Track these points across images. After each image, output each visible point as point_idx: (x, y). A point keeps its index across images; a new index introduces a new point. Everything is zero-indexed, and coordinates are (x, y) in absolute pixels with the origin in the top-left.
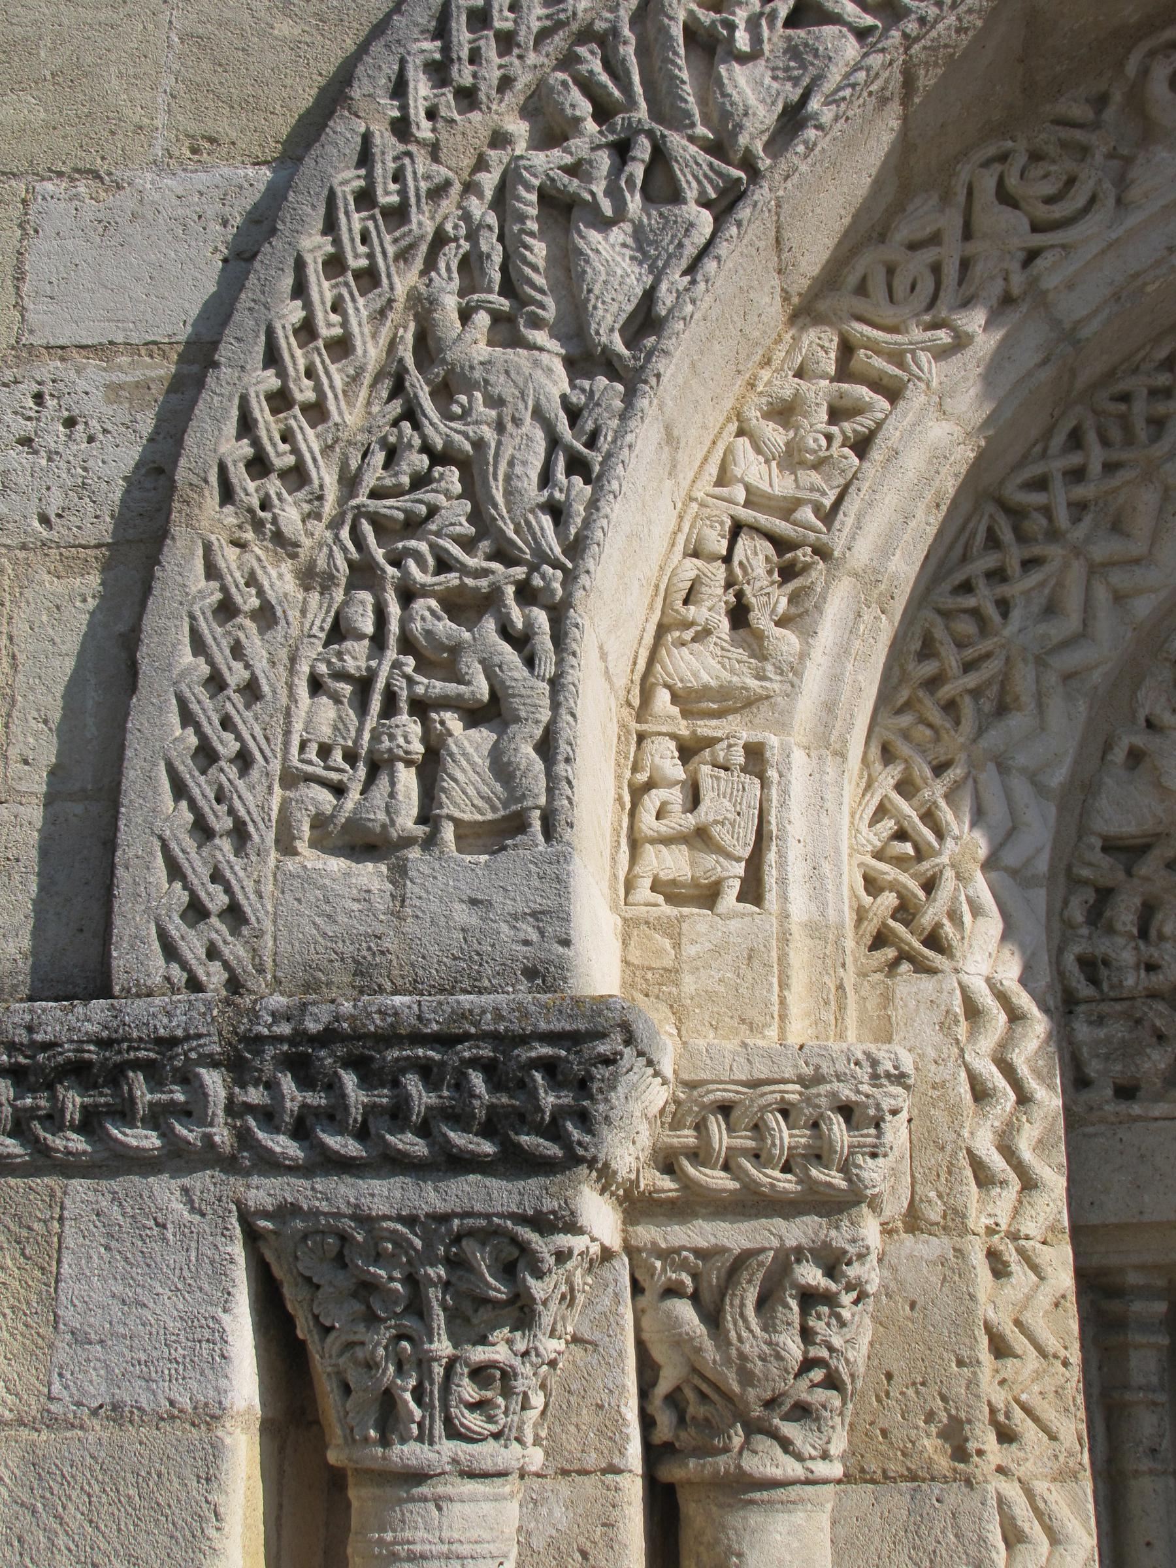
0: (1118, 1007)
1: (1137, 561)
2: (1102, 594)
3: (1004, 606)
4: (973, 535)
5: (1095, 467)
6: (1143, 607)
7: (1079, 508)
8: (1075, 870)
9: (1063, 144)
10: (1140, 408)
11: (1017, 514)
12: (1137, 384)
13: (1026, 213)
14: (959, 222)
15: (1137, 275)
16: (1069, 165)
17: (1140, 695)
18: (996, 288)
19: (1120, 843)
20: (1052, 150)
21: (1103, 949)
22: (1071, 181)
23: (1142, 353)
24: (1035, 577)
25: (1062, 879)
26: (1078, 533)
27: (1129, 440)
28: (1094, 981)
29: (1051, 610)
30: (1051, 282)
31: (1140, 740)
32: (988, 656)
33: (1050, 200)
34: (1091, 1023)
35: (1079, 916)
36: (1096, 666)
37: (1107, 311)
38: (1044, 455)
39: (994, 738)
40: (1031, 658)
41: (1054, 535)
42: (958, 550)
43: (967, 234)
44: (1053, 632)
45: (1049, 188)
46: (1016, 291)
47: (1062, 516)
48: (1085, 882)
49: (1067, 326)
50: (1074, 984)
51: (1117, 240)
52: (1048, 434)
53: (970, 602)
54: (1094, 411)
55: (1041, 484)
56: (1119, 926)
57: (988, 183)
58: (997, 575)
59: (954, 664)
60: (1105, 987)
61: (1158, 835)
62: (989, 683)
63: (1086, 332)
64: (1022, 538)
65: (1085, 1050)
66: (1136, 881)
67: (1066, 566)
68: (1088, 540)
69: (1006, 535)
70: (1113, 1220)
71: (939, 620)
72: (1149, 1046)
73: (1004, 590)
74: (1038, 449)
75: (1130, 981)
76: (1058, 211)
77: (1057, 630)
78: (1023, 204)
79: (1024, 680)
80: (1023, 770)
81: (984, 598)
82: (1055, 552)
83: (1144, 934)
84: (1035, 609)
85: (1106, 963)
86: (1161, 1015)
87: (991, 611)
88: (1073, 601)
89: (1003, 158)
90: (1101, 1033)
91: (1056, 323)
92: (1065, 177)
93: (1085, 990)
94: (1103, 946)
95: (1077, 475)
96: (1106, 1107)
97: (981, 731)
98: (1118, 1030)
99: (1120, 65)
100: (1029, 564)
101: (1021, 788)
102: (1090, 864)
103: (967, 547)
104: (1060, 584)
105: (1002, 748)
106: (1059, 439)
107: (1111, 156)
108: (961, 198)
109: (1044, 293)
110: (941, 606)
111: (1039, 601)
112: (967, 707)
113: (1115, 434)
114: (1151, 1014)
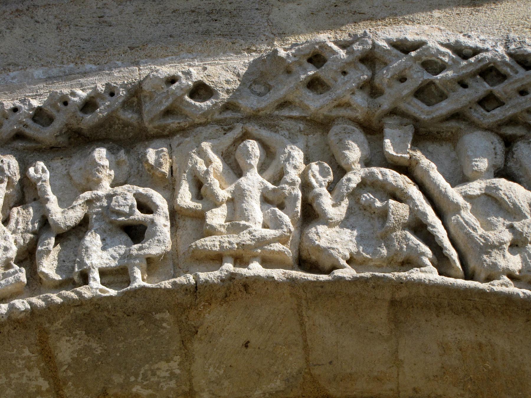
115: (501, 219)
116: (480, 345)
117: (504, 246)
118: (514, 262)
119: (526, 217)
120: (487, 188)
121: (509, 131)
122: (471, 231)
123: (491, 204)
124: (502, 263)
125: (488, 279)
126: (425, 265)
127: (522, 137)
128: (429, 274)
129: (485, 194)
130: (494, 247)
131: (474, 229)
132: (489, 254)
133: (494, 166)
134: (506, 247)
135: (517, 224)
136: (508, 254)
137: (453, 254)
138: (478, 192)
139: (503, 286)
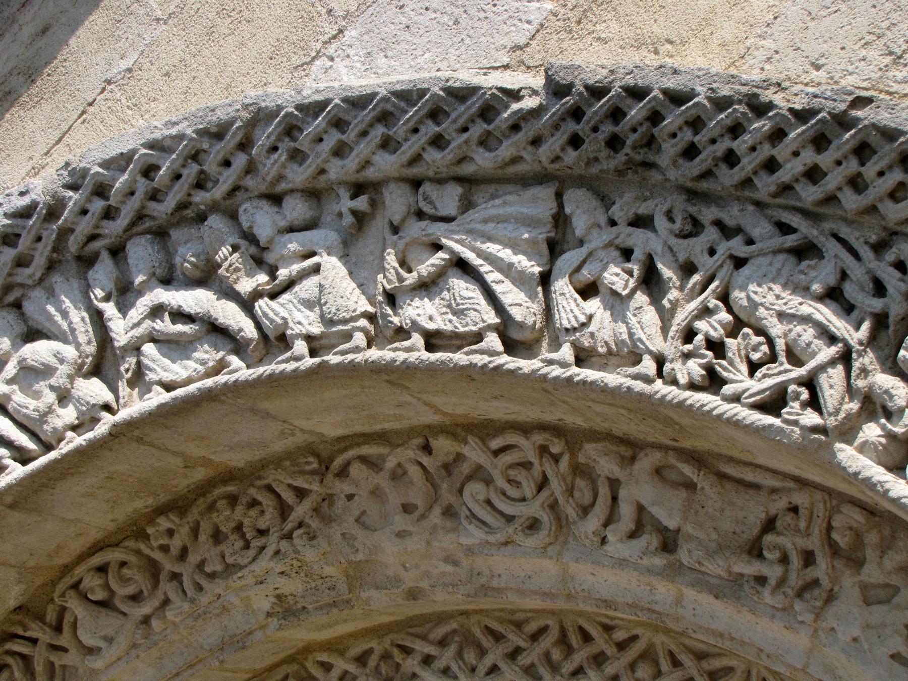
115: (42, 383)
116: (107, 478)
117: (54, 407)
118: (69, 415)
119: (57, 369)
120: (19, 362)
121: (11, 298)
122: (25, 411)
123: (30, 374)
124: (59, 423)
125: (60, 440)
126: (6, 467)
127: (23, 295)
128: (17, 471)
129: (21, 368)
130: (46, 414)
131: (27, 408)
132: (46, 422)
133: (16, 337)
134: (56, 407)
135: (53, 381)
136: (60, 411)
137: (23, 440)
138: (15, 371)
139: (75, 441)
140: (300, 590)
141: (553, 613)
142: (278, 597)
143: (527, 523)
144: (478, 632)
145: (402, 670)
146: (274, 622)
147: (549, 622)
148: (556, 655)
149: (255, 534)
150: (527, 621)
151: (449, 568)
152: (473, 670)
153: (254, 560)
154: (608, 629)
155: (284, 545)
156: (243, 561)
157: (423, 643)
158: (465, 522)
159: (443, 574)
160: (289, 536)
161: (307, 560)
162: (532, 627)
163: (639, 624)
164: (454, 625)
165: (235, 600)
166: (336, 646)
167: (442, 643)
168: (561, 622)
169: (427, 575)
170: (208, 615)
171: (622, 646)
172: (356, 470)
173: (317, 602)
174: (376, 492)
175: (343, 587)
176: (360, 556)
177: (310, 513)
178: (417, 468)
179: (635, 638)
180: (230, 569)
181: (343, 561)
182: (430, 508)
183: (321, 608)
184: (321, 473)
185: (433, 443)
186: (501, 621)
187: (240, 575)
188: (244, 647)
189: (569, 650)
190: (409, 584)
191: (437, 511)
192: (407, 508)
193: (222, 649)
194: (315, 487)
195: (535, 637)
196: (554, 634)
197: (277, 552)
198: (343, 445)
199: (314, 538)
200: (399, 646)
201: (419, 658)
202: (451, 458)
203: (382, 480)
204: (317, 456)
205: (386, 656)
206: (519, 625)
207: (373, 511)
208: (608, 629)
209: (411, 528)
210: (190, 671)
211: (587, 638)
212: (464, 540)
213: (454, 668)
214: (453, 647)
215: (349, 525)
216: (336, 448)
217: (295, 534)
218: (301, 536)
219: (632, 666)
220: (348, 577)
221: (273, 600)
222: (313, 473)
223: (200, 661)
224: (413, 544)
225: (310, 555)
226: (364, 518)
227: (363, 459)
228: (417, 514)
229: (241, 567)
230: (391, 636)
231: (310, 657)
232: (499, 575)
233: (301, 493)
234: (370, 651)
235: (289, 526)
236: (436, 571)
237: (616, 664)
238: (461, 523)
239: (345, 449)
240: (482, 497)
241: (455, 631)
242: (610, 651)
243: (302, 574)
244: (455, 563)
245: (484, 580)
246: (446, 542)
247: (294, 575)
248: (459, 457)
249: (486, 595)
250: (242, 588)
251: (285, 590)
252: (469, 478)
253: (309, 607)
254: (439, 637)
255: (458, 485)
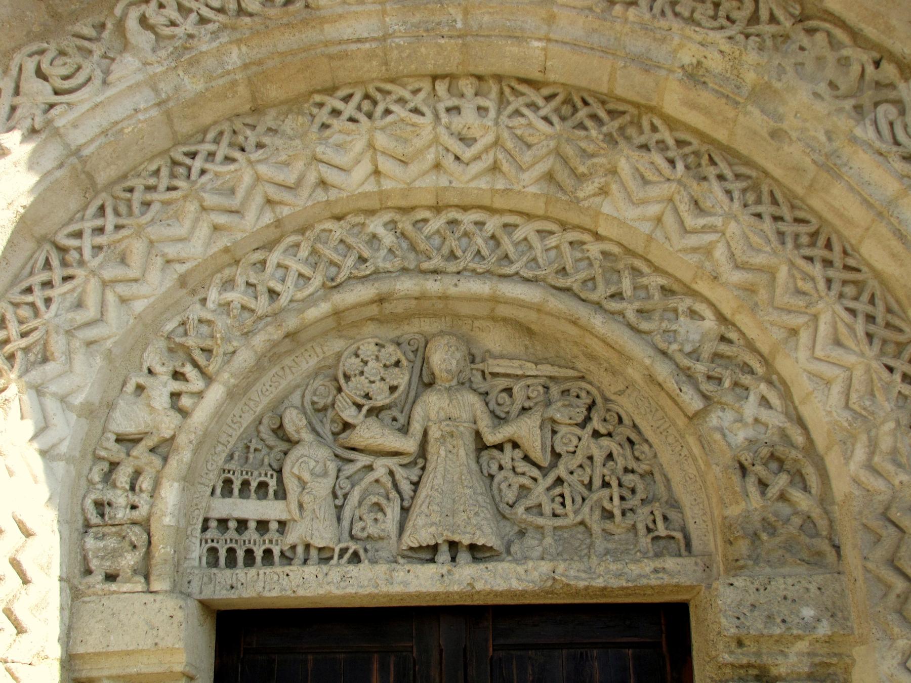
0: (114, 529)
1: (136, 280)
2: (111, 297)
3: (48, 301)
4: (36, 262)
5: (109, 227)
6: (139, 306)
7: (98, 248)
8: (97, 452)
9: (79, 49)
10: (137, 197)
11: (63, 250)
12: (138, 183)
13: (51, 84)
14: (12, 85)
15: (117, 123)
16: (79, 59)
17: (145, 355)
18: (28, 123)
19: (127, 437)
20: (70, 50)
21: (109, 496)
22: (79, 68)
23: (143, 166)
24: (68, 286)
25: (90, 457)
26: (94, 263)
27: (130, 213)
28: (102, 515)
29: (79, 305)
30: (60, 123)
31: (141, 381)
32: (36, 329)
33: (65, 78)
34: (96, 538)
35: (96, 478)
36: (109, 337)
37: (100, 141)
38: (82, 219)
39: (35, 375)
40: (62, 331)
41: (81, 263)
42: (28, 269)
43: (17, 92)
44: (78, 318)
45: (64, 71)
46: (37, 127)
47: (87, 253)
48: (103, 459)
49: (73, 148)
50: (89, 516)
51: (101, 102)
52: (85, 208)
53: (29, 298)
54: (113, 196)
55: (79, 235)
56: (118, 484)
57: (30, 66)
58: (48, 284)
59: (14, 333)
60: (107, 518)
61: (147, 433)
62: (35, 343)
63: (86, 152)
64: (64, 264)
65: (90, 553)
66: (131, 459)
67: (87, 281)
68: (101, 266)
69: (55, 262)
70: (91, 650)
71: (10, 309)
72: (127, 551)
73: (49, 293)
74: (79, 215)
75: (120, 515)
76: (67, 85)
77: (81, 317)
78: (50, 79)
79: (58, 344)
80: (54, 395)
81: (37, 297)
82: (80, 273)
83: (132, 488)
84: (67, 304)
85: (109, 504)
86: (136, 535)
87: (40, 304)
88: (92, 300)
89: (42, 52)
90: (101, 544)
91: (67, 146)
92: (75, 66)
93: (95, 519)
94: (109, 495)
95: (101, 230)
96: (97, 586)
97: (27, 371)
98: (111, 543)
99: (112, 8)
100: (66, 279)
101: (52, 405)
102: (106, 449)
103: (33, 268)
104: (84, 291)
105: (39, 382)
106: (92, 210)
107: (105, 56)
108: (14, 72)
109: (57, 129)
110: (14, 301)
111: (71, 299)
112: (19, 355)
113: (123, 209)
114: (131, 533)
140: (717, 71)
141: (820, 217)
142: (699, 63)
143: (905, 155)
144: (765, 189)
145: (700, 169)
146: (680, 74)
147: (814, 220)
148: (804, 240)
149: (725, 15)
150: (800, 209)
151: (823, 138)
152: (745, 206)
153: (712, 29)
154: (845, 253)
155: (741, 38)
156: (704, 22)
157: (727, 166)
158: (868, 122)
159: (814, 138)
160: (747, 36)
161: (744, 57)
162: (801, 215)
163: (869, 265)
164: (754, 174)
165: (677, 40)
166: (672, 123)
167: (737, 176)
168: (821, 227)
169: (803, 130)
170: (652, 34)
171: (847, 268)
172: (820, 37)
173: (721, 86)
174: (820, 60)
175: (745, 92)
176: (778, 85)
177: (770, 35)
178: (860, 69)
179: (858, 270)
180: (691, 20)
181: (766, 78)
182: (845, 97)
183: (717, 92)
184: (801, 19)
185: (884, 64)
186: (784, 195)
187: (697, 29)
188: (647, 71)
189: (813, 244)
190: (785, 126)
191: (852, 102)
192: (832, 85)
193: (633, 60)
194: (788, 24)
195: (797, 220)
196: (812, 229)
197: (730, 38)
198: (826, 16)
199: (760, 49)
200: (709, 155)
201: (718, 172)
202: (887, 82)
203: (831, 57)
204: (803, 9)
205: (696, 154)
206: (793, 207)
207: (810, 67)
208: (845, 253)
209: (827, 97)
210: (602, 54)
211: (828, 246)
212: (858, 132)
213: (736, 195)
214: (744, 184)
215: (788, 64)
216: (819, 15)
217: (752, 38)
218: (756, 42)
219: (845, 283)
220: (753, 89)
221: (694, 61)
222: (792, 15)
223: (613, 54)
224: (821, 108)
225: (752, 57)
226: (799, 67)
227: (829, 34)
228: (836, 93)
229: (699, 25)
230: (710, 147)
231: (650, 115)
232: (851, 168)
233: (773, 19)
234: (689, 144)
235: (752, 30)
236: (812, 133)
237: (838, 273)
238: (863, 119)
239: (825, 20)
240: (891, 117)
241: (749, 177)
242: (838, 263)
243: (731, 64)
244: (830, 139)
245: (839, 162)
246: (844, 123)
247: (727, 59)
248: (892, 86)
249: (828, 171)
250: (689, 38)
251: (707, 63)
252: (887, 101)
253: (711, 85)
254: (739, 172)
255: (878, 99)
